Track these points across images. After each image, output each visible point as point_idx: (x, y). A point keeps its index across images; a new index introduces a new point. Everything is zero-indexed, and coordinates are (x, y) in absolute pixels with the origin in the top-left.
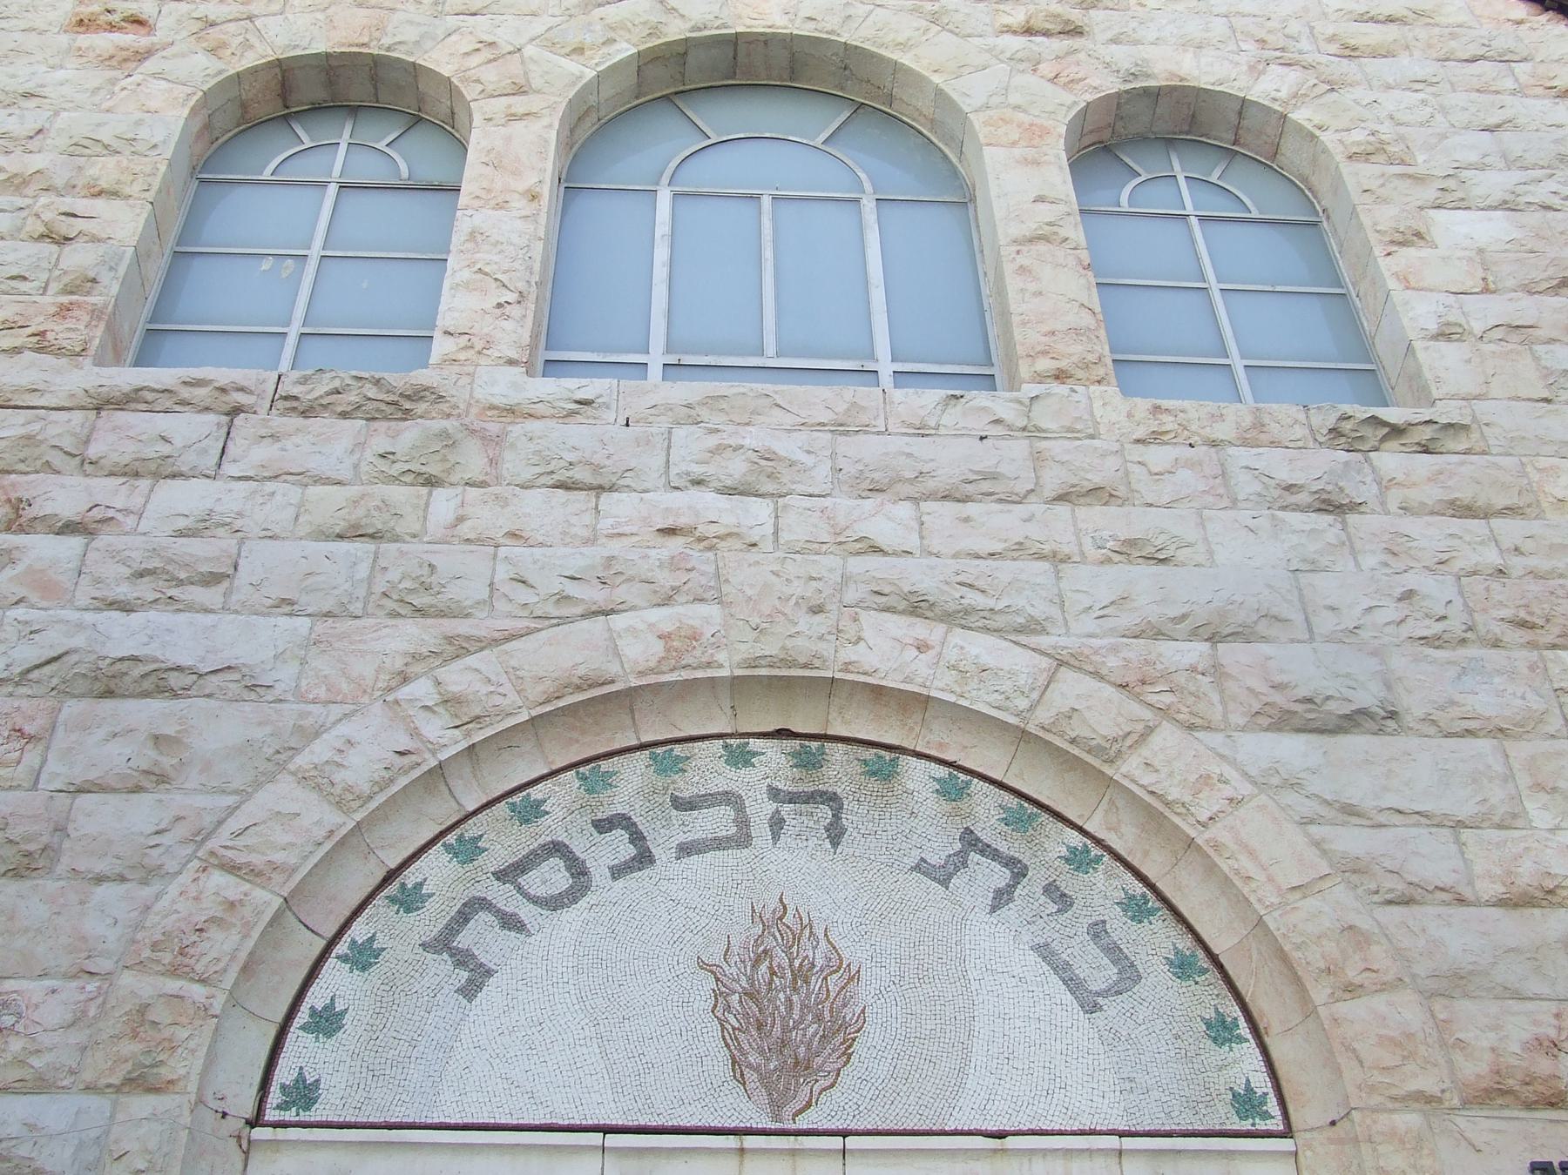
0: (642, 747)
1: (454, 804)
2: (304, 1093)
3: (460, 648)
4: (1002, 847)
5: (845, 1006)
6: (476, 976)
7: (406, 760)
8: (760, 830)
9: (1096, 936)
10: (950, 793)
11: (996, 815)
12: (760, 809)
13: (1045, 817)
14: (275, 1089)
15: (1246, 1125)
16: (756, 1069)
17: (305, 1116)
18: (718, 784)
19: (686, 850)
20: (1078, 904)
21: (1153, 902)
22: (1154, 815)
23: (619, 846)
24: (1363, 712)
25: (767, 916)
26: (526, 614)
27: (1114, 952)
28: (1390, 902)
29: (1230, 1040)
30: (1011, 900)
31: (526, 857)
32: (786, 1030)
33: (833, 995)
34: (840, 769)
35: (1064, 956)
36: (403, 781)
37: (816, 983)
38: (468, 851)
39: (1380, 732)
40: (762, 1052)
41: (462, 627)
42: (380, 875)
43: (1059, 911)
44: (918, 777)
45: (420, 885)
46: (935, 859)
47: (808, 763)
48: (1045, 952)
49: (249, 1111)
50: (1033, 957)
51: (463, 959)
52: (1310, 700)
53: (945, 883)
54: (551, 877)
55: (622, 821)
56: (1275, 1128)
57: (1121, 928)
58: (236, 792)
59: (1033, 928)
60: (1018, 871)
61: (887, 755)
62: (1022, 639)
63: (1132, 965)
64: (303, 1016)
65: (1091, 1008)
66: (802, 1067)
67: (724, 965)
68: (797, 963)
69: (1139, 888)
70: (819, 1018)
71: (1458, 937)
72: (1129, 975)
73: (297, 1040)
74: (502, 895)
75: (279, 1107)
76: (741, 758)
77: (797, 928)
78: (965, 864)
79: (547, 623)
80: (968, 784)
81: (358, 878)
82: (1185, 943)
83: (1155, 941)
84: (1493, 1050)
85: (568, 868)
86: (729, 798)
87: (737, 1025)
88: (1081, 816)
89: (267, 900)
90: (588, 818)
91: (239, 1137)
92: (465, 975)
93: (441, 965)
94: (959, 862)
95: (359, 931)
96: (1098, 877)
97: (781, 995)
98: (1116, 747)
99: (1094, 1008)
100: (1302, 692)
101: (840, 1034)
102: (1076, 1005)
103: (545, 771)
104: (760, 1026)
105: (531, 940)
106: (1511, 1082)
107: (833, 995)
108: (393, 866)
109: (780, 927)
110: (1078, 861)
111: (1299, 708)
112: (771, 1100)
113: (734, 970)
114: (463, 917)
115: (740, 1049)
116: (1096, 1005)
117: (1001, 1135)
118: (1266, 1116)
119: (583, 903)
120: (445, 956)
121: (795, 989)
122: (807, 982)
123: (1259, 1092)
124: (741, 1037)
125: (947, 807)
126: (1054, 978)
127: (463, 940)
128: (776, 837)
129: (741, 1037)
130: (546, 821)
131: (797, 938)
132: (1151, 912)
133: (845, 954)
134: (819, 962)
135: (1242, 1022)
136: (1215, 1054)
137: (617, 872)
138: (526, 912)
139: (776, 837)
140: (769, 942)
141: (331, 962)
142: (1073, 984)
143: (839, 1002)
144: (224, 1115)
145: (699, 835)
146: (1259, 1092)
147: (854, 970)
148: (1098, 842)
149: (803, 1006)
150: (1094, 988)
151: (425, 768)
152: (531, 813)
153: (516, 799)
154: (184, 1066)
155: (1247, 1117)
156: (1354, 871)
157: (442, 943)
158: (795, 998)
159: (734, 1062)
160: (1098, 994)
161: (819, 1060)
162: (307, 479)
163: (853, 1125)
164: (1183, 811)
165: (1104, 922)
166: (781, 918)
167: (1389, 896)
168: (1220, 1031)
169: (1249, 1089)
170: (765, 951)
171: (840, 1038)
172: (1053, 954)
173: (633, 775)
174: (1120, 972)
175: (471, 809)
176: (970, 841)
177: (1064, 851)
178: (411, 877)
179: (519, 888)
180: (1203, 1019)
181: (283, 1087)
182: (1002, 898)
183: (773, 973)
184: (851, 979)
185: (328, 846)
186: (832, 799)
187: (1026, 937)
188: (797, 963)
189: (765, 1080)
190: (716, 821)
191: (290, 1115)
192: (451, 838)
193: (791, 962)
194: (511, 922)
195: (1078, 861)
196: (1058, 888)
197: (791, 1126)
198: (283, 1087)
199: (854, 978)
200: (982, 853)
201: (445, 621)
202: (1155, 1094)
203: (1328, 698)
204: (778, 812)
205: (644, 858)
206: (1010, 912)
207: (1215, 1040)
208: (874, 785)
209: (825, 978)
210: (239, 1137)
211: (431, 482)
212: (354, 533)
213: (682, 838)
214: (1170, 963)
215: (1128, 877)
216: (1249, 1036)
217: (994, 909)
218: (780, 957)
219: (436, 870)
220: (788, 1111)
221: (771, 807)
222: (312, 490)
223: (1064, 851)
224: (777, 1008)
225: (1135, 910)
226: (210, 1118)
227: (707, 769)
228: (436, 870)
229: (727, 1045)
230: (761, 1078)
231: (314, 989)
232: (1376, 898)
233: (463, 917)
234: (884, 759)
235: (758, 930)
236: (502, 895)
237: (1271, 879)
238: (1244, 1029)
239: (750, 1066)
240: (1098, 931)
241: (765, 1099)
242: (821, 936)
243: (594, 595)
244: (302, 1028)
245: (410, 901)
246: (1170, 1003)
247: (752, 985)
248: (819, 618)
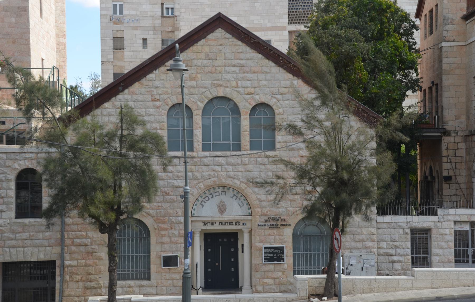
2: (194, 214)
3: (199, 183)
6: (203, 206)
10: (233, 191)
12: (220, 193)
22: (246, 194)
23: (211, 196)
34: (226, 189)
38: (201, 197)
44: (231, 189)
47: (224, 188)
51: (202, 205)
54: (207, 199)
60: (237, 197)
66: (223, 212)
72: (243, 205)
74: (204, 200)
76: (219, 188)
83: (246, 202)
86: (218, 192)
93: (201, 205)
101: (225, 209)
109: (221, 202)
110: (241, 196)
157: (201, 204)
168: (249, 209)
173: (212, 190)
176: (234, 195)
182: (236, 199)
190: (217, 194)
194: (205, 202)
195: (241, 196)
205: (213, 197)
219: (200, 198)
227: (217, 190)
228: (200, 198)
234: (229, 188)
236: (204, 200)
245: (198, 201)
246: (246, 207)
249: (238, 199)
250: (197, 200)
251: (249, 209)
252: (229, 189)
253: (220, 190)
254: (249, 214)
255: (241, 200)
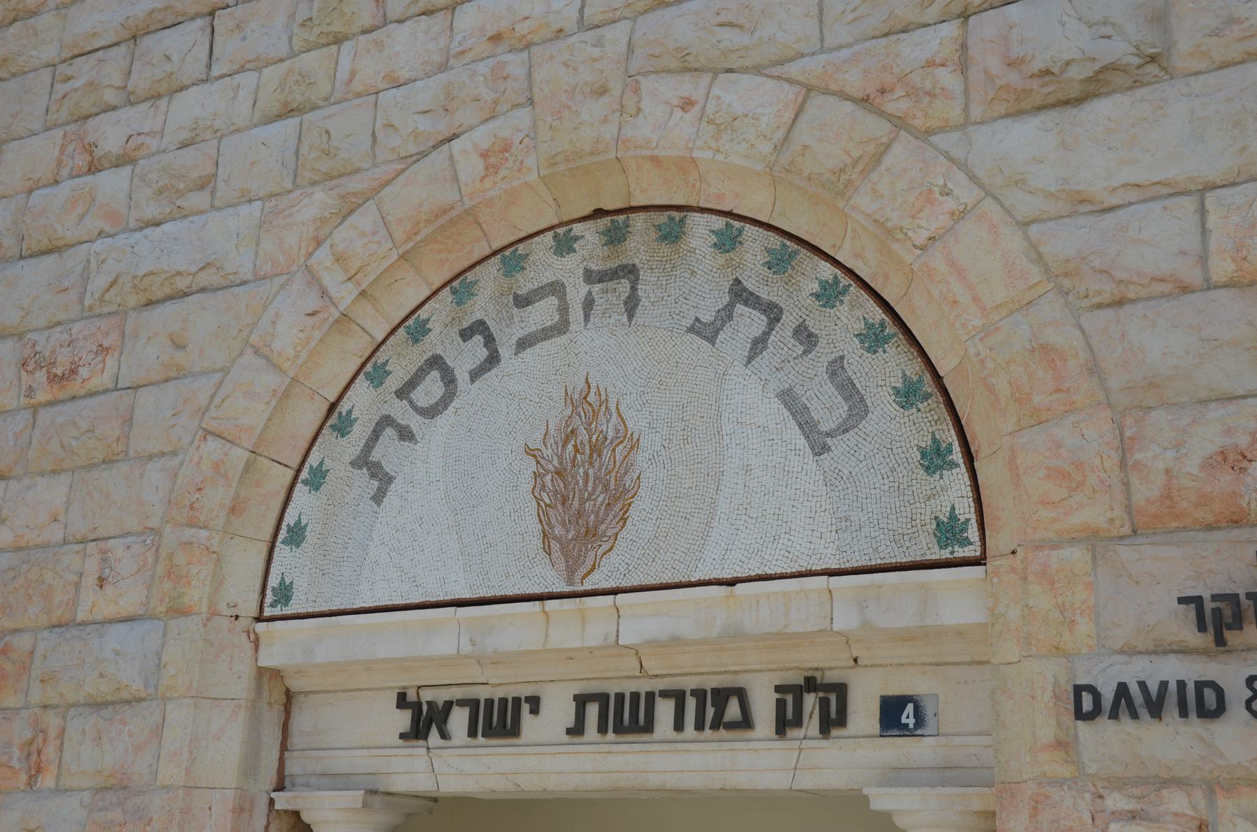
0: (495, 253)
1: (367, 337)
4: (763, 293)
5: (626, 473)
7: (317, 318)
8: (576, 313)
9: (833, 375)
10: (727, 243)
11: (763, 258)
12: (577, 292)
13: (804, 252)
14: (269, 592)
15: (945, 554)
16: (559, 540)
17: (288, 611)
18: (547, 277)
19: (523, 344)
20: (822, 342)
21: (891, 328)
23: (476, 350)
24: (1113, 67)
25: (576, 397)
26: (395, 156)
27: (848, 390)
28: (1099, 306)
29: (941, 467)
30: (765, 348)
31: (416, 374)
32: (583, 501)
33: (618, 464)
35: (803, 399)
36: (318, 335)
37: (607, 454)
38: (379, 377)
39: (1137, 84)
40: (563, 524)
41: (354, 185)
42: (324, 408)
43: (805, 352)
44: (701, 230)
45: (350, 412)
46: (707, 317)
47: (615, 238)
48: (787, 398)
49: (254, 612)
50: (776, 404)
51: (375, 470)
52: (1048, 72)
53: (712, 340)
54: (432, 388)
55: (480, 327)
56: (972, 554)
57: (859, 364)
58: (221, 370)
59: (780, 375)
60: (773, 313)
61: (676, 215)
62: (776, 71)
63: (862, 400)
64: (283, 534)
65: (820, 449)
66: (591, 535)
67: (543, 448)
68: (594, 437)
69: (878, 314)
70: (606, 488)
71: (1157, 340)
72: (858, 407)
73: (281, 551)
74: (402, 413)
75: (272, 606)
76: (565, 246)
77: (596, 405)
78: (730, 318)
79: (410, 160)
80: (740, 232)
81: (307, 415)
82: (914, 368)
84: (1167, 471)
85: (442, 379)
86: (556, 289)
87: (548, 502)
88: (834, 246)
89: (239, 456)
90: (456, 330)
91: (248, 632)
92: (376, 484)
94: (726, 314)
95: (313, 460)
96: (843, 310)
97: (581, 471)
98: (844, 177)
99: (825, 449)
100: (1037, 65)
101: (620, 498)
102: (808, 449)
103: (428, 293)
104: (564, 501)
105: (417, 447)
106: (1184, 504)
107: (618, 464)
108: (332, 399)
109: (586, 404)
110: (828, 295)
111: (1035, 84)
112: (567, 566)
113: (550, 452)
114: (376, 435)
115: (549, 523)
116: (825, 444)
117: (732, 583)
118: (966, 542)
119: (451, 409)
120: (365, 470)
121: (591, 464)
122: (600, 456)
123: (962, 519)
124: (551, 512)
125: (721, 259)
126: (792, 424)
127: (375, 456)
128: (587, 318)
129: (551, 512)
130: (431, 337)
131: (596, 414)
132: (886, 340)
133: (630, 425)
134: (611, 435)
135: (956, 448)
136: (924, 482)
137: (475, 375)
138: (414, 421)
139: (587, 318)
140: (576, 422)
141: (299, 486)
142: (807, 426)
143: (622, 471)
144: (237, 617)
145: (533, 329)
146: (962, 519)
147: (635, 437)
148: (850, 272)
149: (596, 478)
150: (824, 427)
151: (331, 320)
152: (419, 332)
153: (410, 322)
154: (196, 595)
155: (946, 546)
156: (1066, 275)
157: (363, 461)
158: (591, 472)
159: (545, 535)
160: (829, 434)
161: (603, 527)
162: (259, 64)
163: (625, 583)
164: (901, 236)
165: (842, 358)
166: (585, 398)
167: (1096, 300)
168: (934, 460)
169: (953, 516)
170: (572, 432)
171: (619, 505)
172: (794, 398)
174: (850, 409)
175: (380, 338)
176: (739, 293)
177: (816, 287)
178: (344, 407)
179: (411, 403)
180: (919, 448)
181: (274, 589)
182: (759, 345)
183: (577, 451)
184: (632, 448)
185: (273, 403)
186: (630, 272)
187: (772, 385)
188: (594, 437)
189: (564, 548)
190: (543, 313)
191: (277, 611)
192: (369, 367)
193: (590, 438)
194: (406, 434)
195: (828, 295)
196: (806, 328)
197: (579, 588)
198: (274, 589)
199: (635, 446)
200: (746, 303)
201: (342, 181)
202: (866, 530)
203: (1068, 63)
204: (590, 293)
206: (763, 361)
207: (928, 468)
208: (665, 249)
209: (614, 450)
210: (248, 632)
211: (339, 40)
212: (288, 111)
213: (521, 334)
214: (897, 392)
215: (870, 304)
216: (961, 461)
217: (750, 359)
218: (583, 434)
220: (577, 578)
221: (584, 289)
222: (266, 71)
223: (816, 287)
224: (577, 483)
225: (872, 340)
226: (225, 623)
229: (541, 521)
230: (562, 549)
231: (289, 510)
232: (1085, 303)
233: (376, 435)
235: (568, 412)
237: (976, 299)
238: (957, 456)
239: (555, 538)
240: (836, 369)
241: (562, 566)
242: (613, 410)
243: (442, 127)
244: (283, 542)
246: (900, 430)
247: (561, 463)
248: (605, 99)
249: (784, 333)
250: (334, 415)
251: (934, 460)
252: (672, 236)
253: (569, 269)
254: (949, 530)
255: (824, 354)
